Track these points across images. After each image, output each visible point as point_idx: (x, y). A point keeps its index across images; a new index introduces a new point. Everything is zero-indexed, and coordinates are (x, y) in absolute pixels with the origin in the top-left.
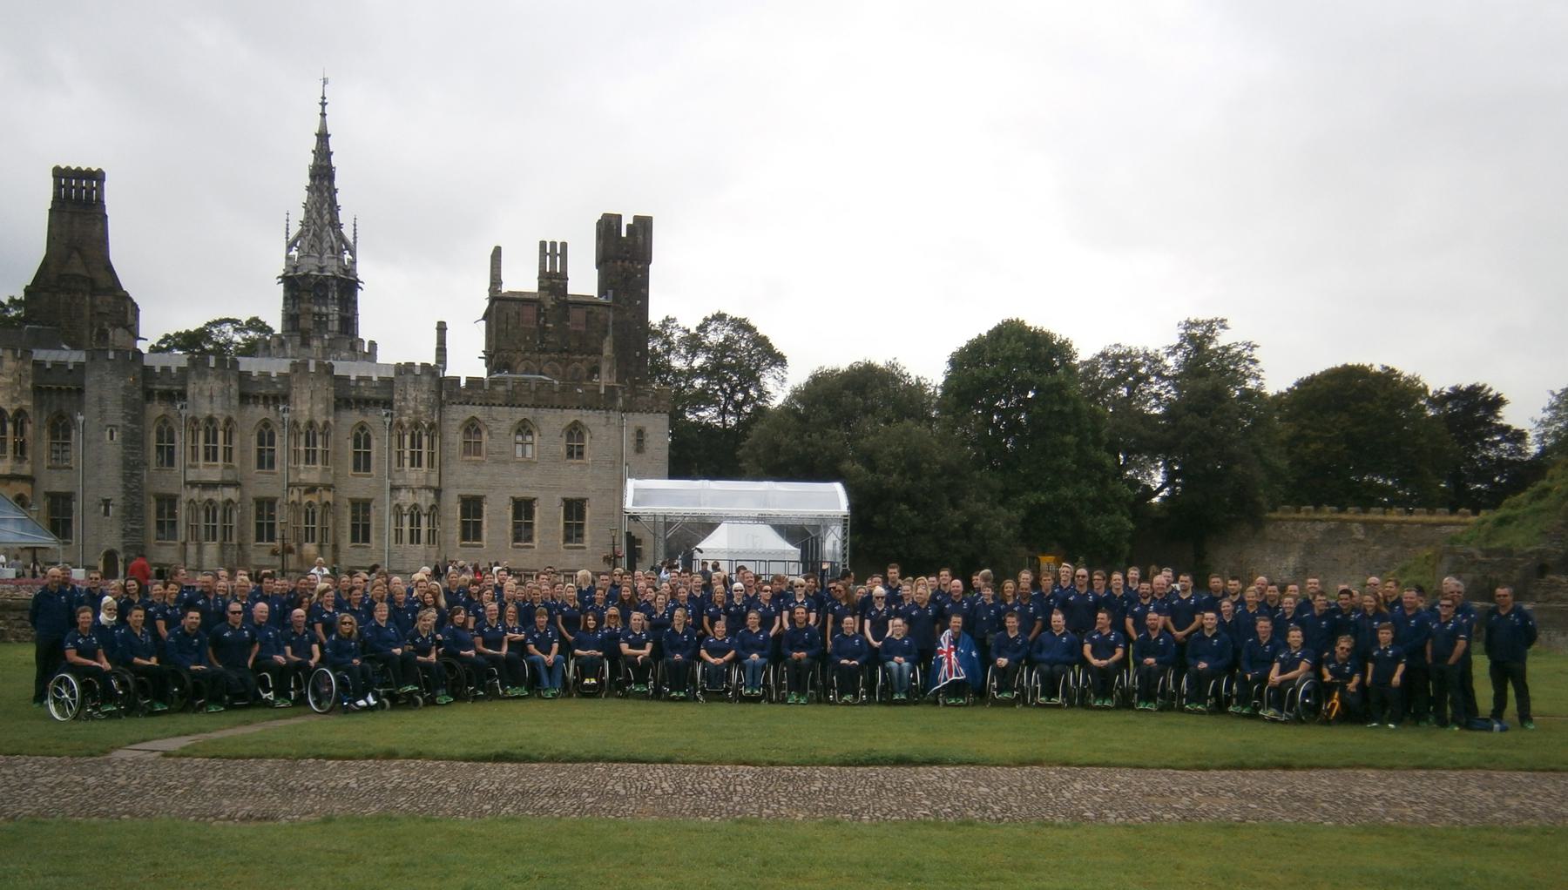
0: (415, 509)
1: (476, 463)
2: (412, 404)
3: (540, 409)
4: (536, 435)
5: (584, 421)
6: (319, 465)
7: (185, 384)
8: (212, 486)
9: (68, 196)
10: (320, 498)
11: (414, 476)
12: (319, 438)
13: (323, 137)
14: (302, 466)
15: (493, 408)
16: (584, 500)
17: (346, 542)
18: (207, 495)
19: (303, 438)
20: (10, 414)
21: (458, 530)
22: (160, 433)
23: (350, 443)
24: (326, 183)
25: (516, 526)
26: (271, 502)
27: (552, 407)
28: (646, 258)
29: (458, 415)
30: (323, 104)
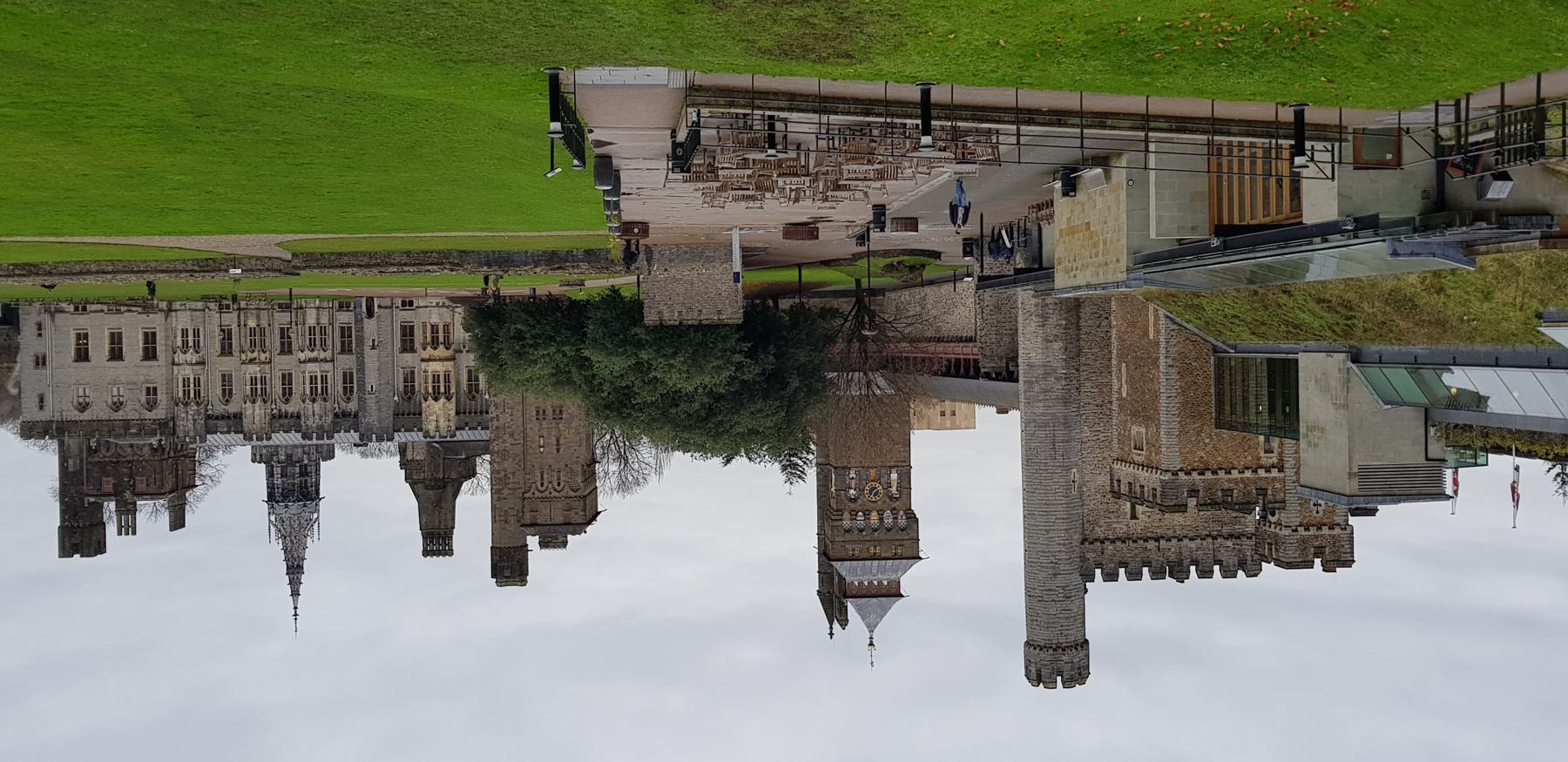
1: (147, 381)
2: (190, 417)
3: (108, 418)
4: (110, 402)
5: (77, 413)
8: (311, 360)
10: (247, 356)
11: (187, 372)
12: (248, 393)
14: (259, 375)
15: (137, 418)
17: (234, 327)
19: (259, 392)
20: (430, 398)
21: (158, 338)
23: (234, 392)
24: (290, 564)
25: (120, 342)
26: (282, 352)
27: (99, 421)
29: (160, 413)
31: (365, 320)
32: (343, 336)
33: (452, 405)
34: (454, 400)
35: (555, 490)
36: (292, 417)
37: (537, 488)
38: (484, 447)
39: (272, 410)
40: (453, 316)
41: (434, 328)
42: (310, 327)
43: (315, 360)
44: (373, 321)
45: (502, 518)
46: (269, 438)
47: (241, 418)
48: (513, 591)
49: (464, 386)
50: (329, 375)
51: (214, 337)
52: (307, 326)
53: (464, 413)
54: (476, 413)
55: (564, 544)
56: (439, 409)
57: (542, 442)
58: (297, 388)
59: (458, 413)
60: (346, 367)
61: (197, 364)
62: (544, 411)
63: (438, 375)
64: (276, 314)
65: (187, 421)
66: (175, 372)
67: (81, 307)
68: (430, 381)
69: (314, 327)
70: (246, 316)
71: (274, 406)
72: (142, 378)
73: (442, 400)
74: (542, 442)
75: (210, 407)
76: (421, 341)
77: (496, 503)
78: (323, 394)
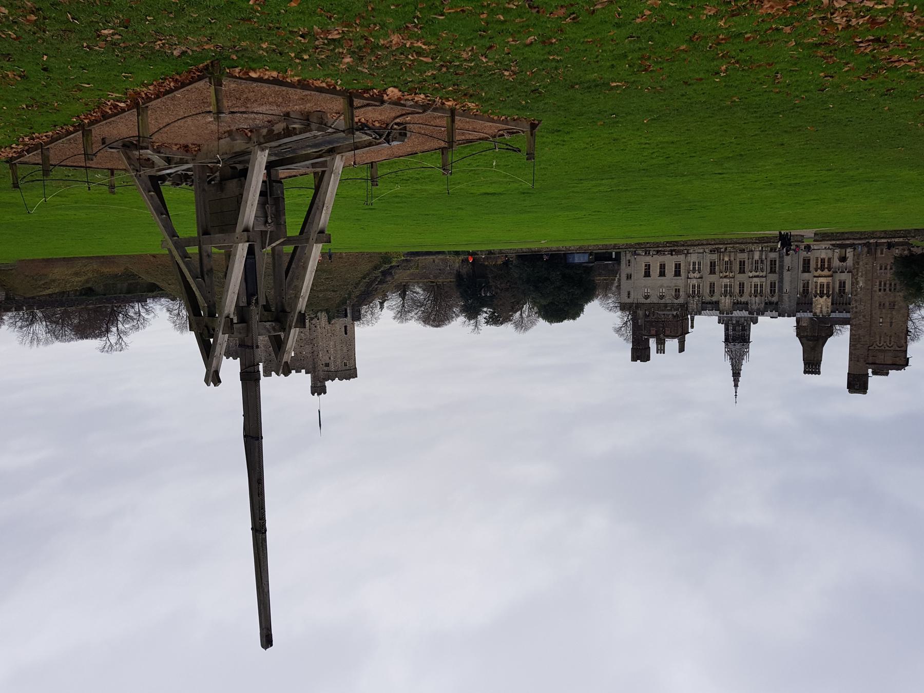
0: (694, 271)
2: (695, 303)
7: (765, 307)
8: (755, 277)
9: (816, 366)
11: (694, 282)
12: (723, 292)
13: (736, 386)
14: (728, 284)
16: (644, 277)
18: (757, 274)
19: (728, 292)
21: (681, 266)
22: (775, 292)
23: (715, 291)
26: (740, 273)
28: (634, 350)
29: (681, 301)
30: (736, 395)
31: (785, 256)
32: (771, 264)
33: (830, 300)
34: (831, 297)
35: (888, 346)
36: (744, 303)
37: (877, 345)
38: (844, 322)
39: (734, 300)
40: (833, 254)
41: (823, 260)
42: (756, 261)
43: (757, 277)
44: (789, 257)
45: (856, 359)
46: (732, 314)
47: (718, 304)
48: (858, 396)
49: (837, 290)
50: (764, 284)
51: (707, 265)
52: (754, 260)
53: (836, 304)
54: (843, 304)
55: (887, 374)
56: (823, 301)
57: (881, 321)
58: (747, 290)
59: (832, 304)
60: (772, 280)
61: (699, 278)
62: (884, 304)
63: (823, 285)
64: (738, 254)
65: (693, 303)
66: (689, 282)
67: (647, 253)
68: (818, 287)
69: (758, 261)
70: (723, 256)
71: (735, 298)
72: (673, 285)
73: (825, 297)
74: (881, 321)
75: (704, 298)
76: (815, 267)
77: (852, 351)
78: (760, 293)
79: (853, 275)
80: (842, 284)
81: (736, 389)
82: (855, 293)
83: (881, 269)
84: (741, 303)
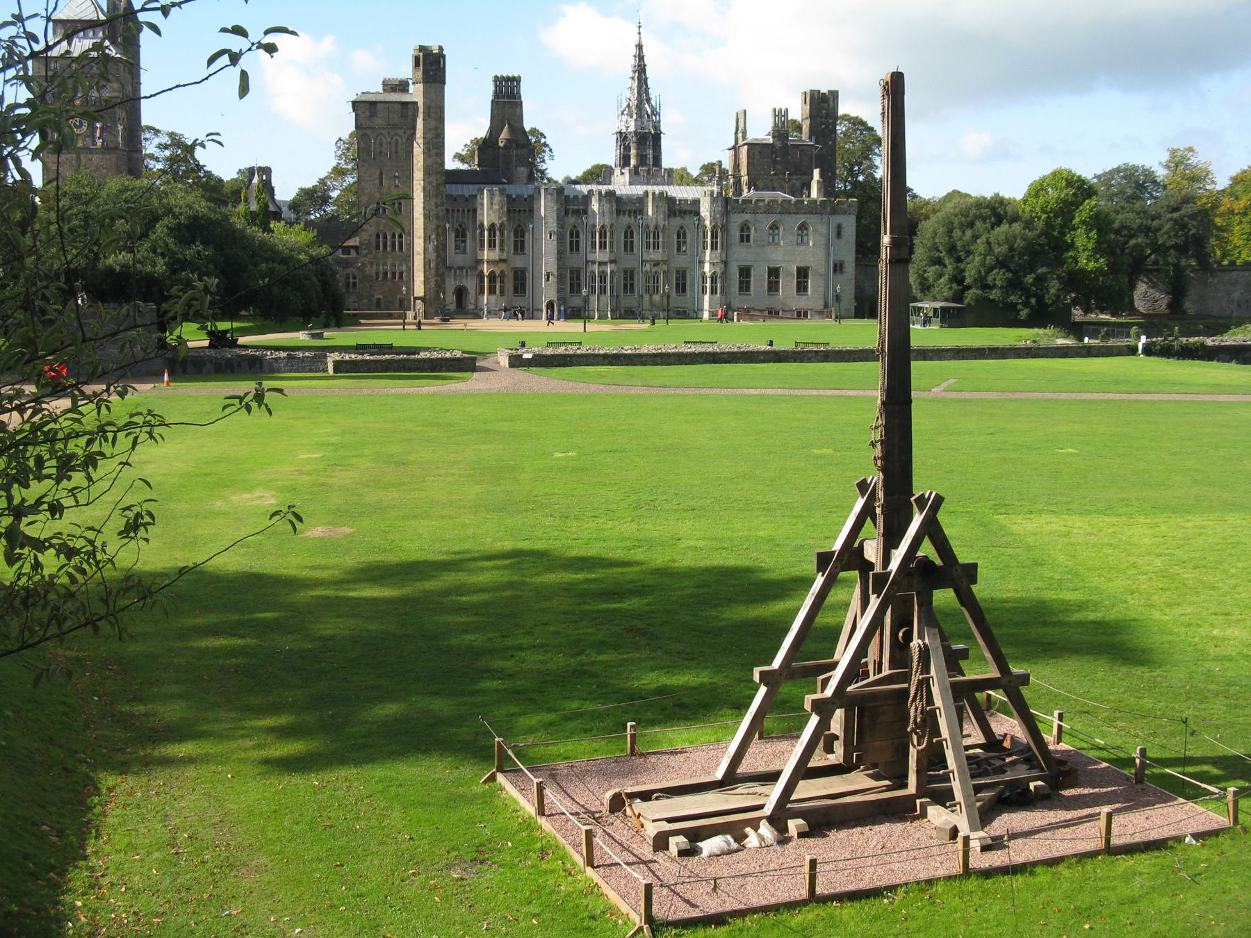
5: (808, 221)
6: (661, 250)
12: (661, 235)
14: (651, 250)
23: (675, 236)
25: (770, 283)
30: (640, 27)
31: (556, 299)
34: (478, 224)
35: (384, 136)
38: (455, 177)
54: (458, 210)
57: (397, 181)
64: (636, 304)
68: (497, 242)
69: (601, 293)
71: (641, 221)
74: (397, 181)
76: (506, 279)
79: (445, 264)
80: (460, 248)
81: (640, 41)
82: (440, 231)
83: (401, 274)
84: (630, 212)
